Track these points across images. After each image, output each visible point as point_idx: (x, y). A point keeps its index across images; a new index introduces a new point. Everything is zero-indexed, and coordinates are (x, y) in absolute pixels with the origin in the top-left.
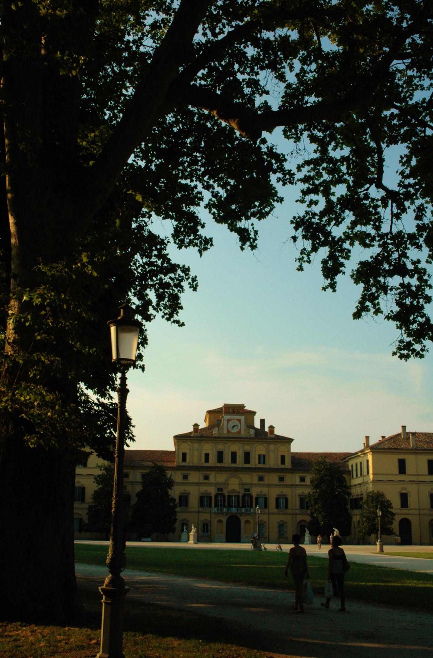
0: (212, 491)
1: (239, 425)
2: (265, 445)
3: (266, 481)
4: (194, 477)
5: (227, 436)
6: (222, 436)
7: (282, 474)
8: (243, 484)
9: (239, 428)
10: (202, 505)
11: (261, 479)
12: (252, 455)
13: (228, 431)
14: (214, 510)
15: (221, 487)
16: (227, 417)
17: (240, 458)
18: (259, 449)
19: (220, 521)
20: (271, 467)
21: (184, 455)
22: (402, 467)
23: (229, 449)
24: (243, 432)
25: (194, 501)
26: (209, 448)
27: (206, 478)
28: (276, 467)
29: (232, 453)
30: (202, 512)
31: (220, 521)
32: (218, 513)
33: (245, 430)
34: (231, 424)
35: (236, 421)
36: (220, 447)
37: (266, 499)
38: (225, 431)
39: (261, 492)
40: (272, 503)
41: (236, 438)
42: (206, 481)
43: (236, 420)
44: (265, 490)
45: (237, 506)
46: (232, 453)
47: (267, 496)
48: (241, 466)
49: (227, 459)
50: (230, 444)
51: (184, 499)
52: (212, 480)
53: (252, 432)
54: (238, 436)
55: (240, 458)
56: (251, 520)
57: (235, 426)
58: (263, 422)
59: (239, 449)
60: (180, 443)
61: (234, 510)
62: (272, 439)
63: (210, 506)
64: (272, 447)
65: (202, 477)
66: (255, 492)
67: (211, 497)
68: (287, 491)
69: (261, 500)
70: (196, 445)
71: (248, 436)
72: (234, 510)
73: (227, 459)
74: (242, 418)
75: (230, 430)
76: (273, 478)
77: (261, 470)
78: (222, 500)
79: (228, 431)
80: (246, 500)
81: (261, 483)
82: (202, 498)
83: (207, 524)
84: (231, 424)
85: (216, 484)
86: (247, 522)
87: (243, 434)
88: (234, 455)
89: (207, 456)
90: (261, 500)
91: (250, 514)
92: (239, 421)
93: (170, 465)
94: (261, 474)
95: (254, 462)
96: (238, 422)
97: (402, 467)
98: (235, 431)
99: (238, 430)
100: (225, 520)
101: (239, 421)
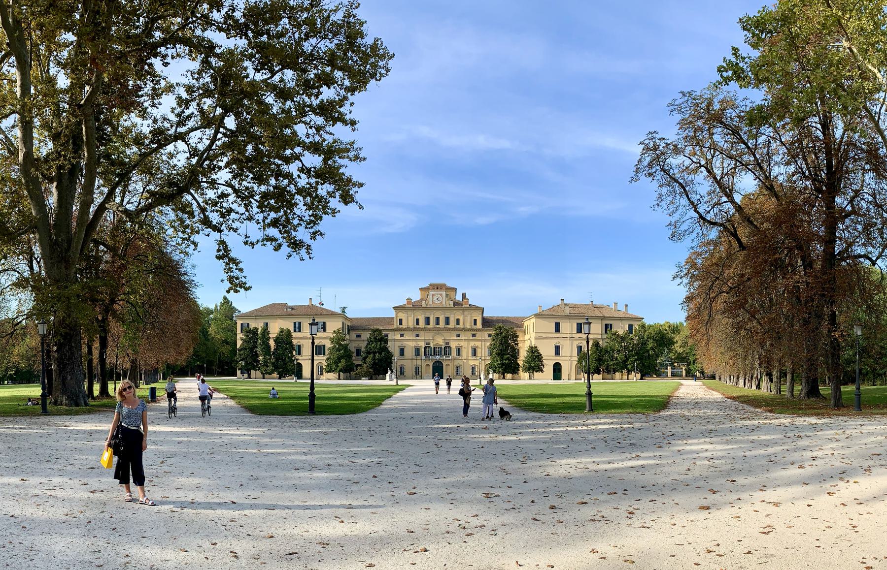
0: (422, 344)
7: (474, 333)
14: (424, 357)
16: (431, 293)
19: (428, 365)
21: (401, 320)
22: (557, 326)
24: (444, 303)
27: (417, 336)
31: (428, 365)
34: (435, 298)
38: (431, 303)
40: (466, 352)
44: (462, 343)
45: (440, 354)
51: (402, 352)
53: (452, 303)
58: (464, 295)
64: (466, 313)
66: (453, 345)
68: (478, 344)
70: (409, 313)
74: (444, 293)
76: (469, 336)
78: (429, 351)
80: (447, 350)
88: (438, 319)
89: (418, 320)
93: (391, 327)
94: (458, 332)
95: (452, 324)
97: (557, 326)
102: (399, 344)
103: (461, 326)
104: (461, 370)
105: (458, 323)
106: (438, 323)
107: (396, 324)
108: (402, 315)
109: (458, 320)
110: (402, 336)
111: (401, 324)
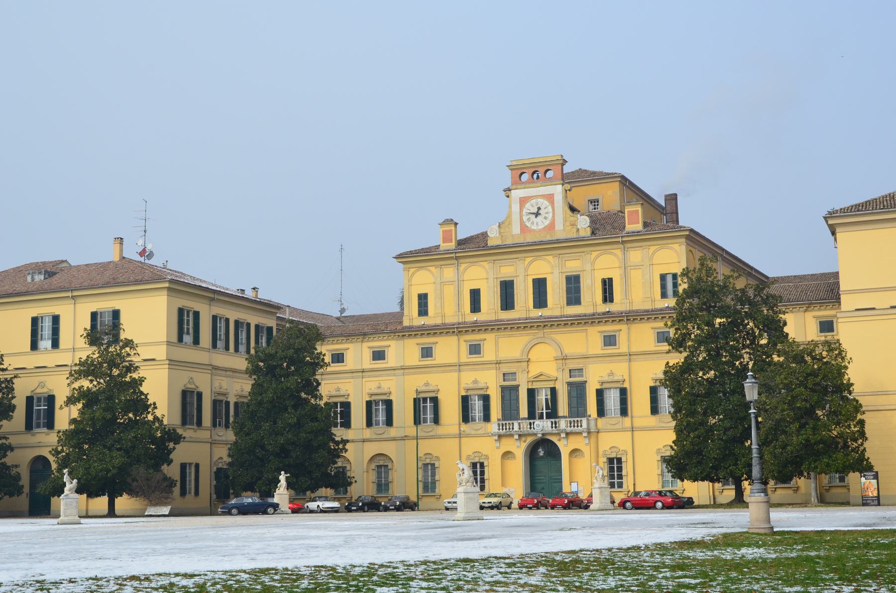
1: (550, 209)
2: (619, 252)
3: (622, 346)
4: (448, 349)
5: (521, 240)
6: (509, 242)
8: (565, 358)
9: (551, 215)
10: (466, 417)
11: (610, 341)
12: (585, 284)
13: (524, 228)
15: (514, 370)
17: (556, 293)
18: (598, 265)
20: (635, 308)
21: (423, 299)
23: (524, 272)
24: (559, 226)
25: (450, 410)
26: (482, 275)
27: (475, 349)
28: (648, 306)
29: (534, 281)
30: (469, 436)
31: (507, 455)
32: (500, 436)
33: (565, 221)
35: (540, 200)
36: (507, 271)
37: (623, 392)
39: (611, 374)
41: (541, 243)
42: (475, 359)
43: (543, 196)
46: (534, 281)
47: (626, 385)
48: (557, 313)
49: (524, 295)
50: (528, 260)
52: (488, 353)
53: (583, 222)
54: (548, 238)
55: (556, 293)
56: (586, 449)
57: (537, 214)
59: (553, 270)
60: (412, 270)
61: (543, 426)
62: (634, 234)
63: (487, 418)
64: (636, 255)
65: (465, 348)
67: (486, 399)
69: (612, 400)
71: (574, 235)
72: (543, 426)
73: (524, 295)
74: (558, 190)
75: (528, 224)
77: (608, 318)
79: (524, 228)
81: (610, 350)
82: (465, 401)
83: (482, 465)
84: (530, 207)
85: (498, 363)
86: (574, 452)
87: (561, 231)
90: (612, 400)
91: (580, 433)
92: (550, 198)
94: (609, 328)
96: (546, 203)
98: (541, 227)
99: (547, 222)
100: (519, 449)
101: (550, 198)
102: (415, 383)
103: (619, 305)
104: (627, 469)
105: (608, 294)
106: (540, 300)
107: (411, 317)
108: (424, 280)
109: (607, 286)
110: (427, 352)
111: (423, 310)
